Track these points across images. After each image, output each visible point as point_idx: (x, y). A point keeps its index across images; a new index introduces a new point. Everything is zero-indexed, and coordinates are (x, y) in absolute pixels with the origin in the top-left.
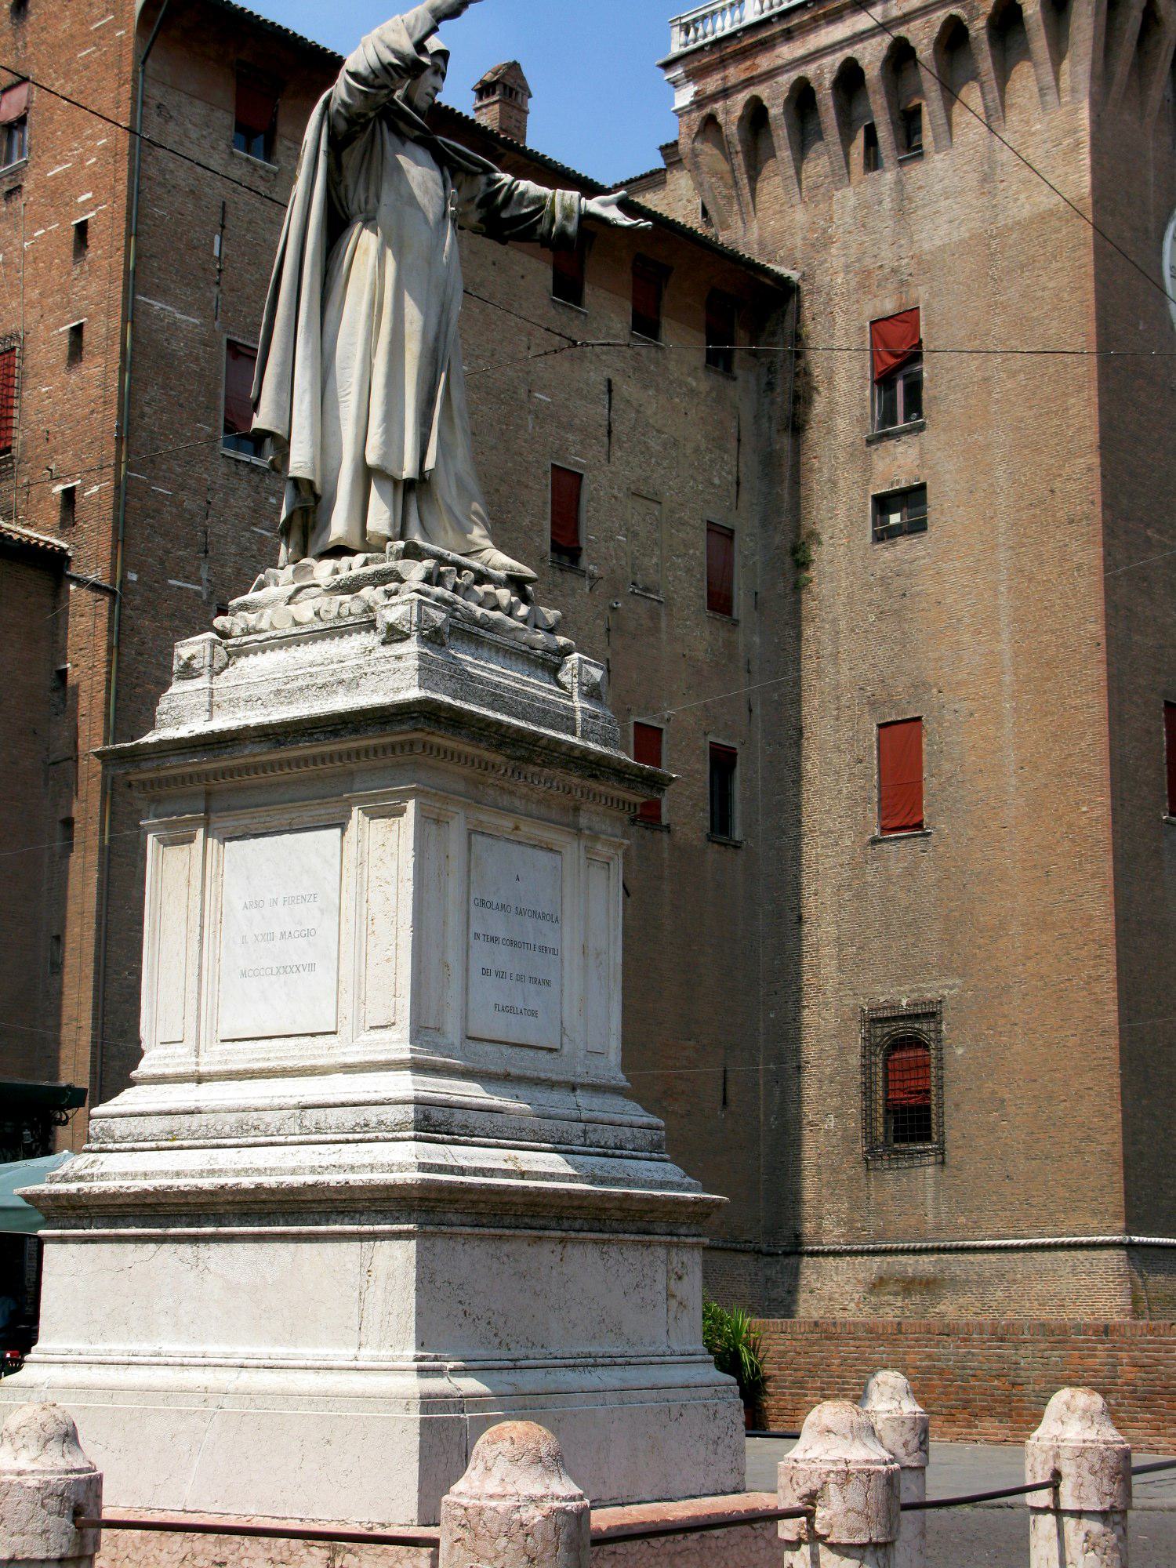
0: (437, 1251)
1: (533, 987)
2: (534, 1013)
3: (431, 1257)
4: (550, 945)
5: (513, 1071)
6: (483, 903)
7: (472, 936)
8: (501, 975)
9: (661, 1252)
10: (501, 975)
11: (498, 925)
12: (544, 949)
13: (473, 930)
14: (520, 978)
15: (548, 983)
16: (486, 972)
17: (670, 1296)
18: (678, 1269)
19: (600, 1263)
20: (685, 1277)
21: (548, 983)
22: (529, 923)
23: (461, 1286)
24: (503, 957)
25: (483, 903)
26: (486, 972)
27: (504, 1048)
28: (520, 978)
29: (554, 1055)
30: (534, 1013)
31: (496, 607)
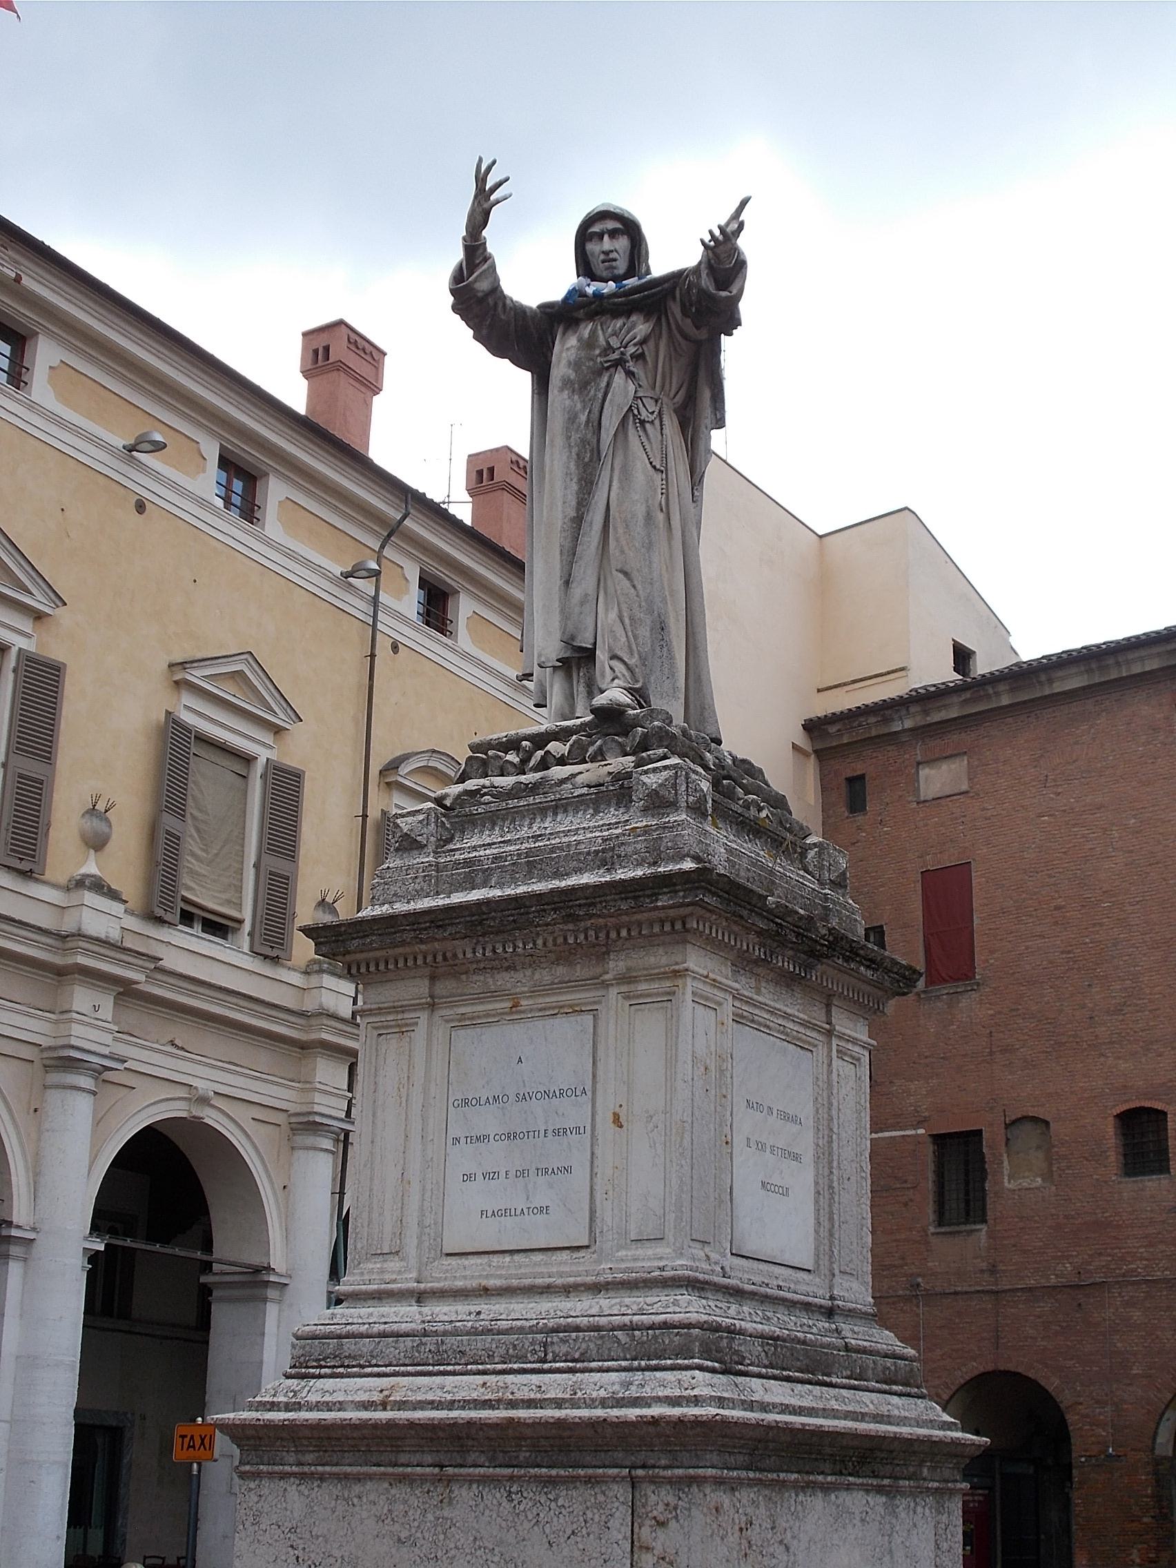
0: (266, 1491)
1: (542, 1180)
2: (543, 1210)
3: (256, 1499)
4: (570, 1124)
5: (492, 1283)
6: (466, 1102)
7: (450, 1141)
8: (490, 1176)
9: (621, 1492)
10: (490, 1176)
11: (488, 1121)
12: (560, 1132)
13: (452, 1133)
14: (522, 1173)
15: (568, 1170)
16: (468, 1177)
17: (636, 1546)
18: (659, 1512)
19: (505, 1503)
20: (673, 1524)
21: (568, 1170)
22: (537, 1106)
23: (293, 1530)
24: (496, 1156)
25: (466, 1102)
26: (468, 1177)
27: (495, 1259)
28: (522, 1173)
29: (582, 1253)
30: (543, 1210)
31: (562, 761)
